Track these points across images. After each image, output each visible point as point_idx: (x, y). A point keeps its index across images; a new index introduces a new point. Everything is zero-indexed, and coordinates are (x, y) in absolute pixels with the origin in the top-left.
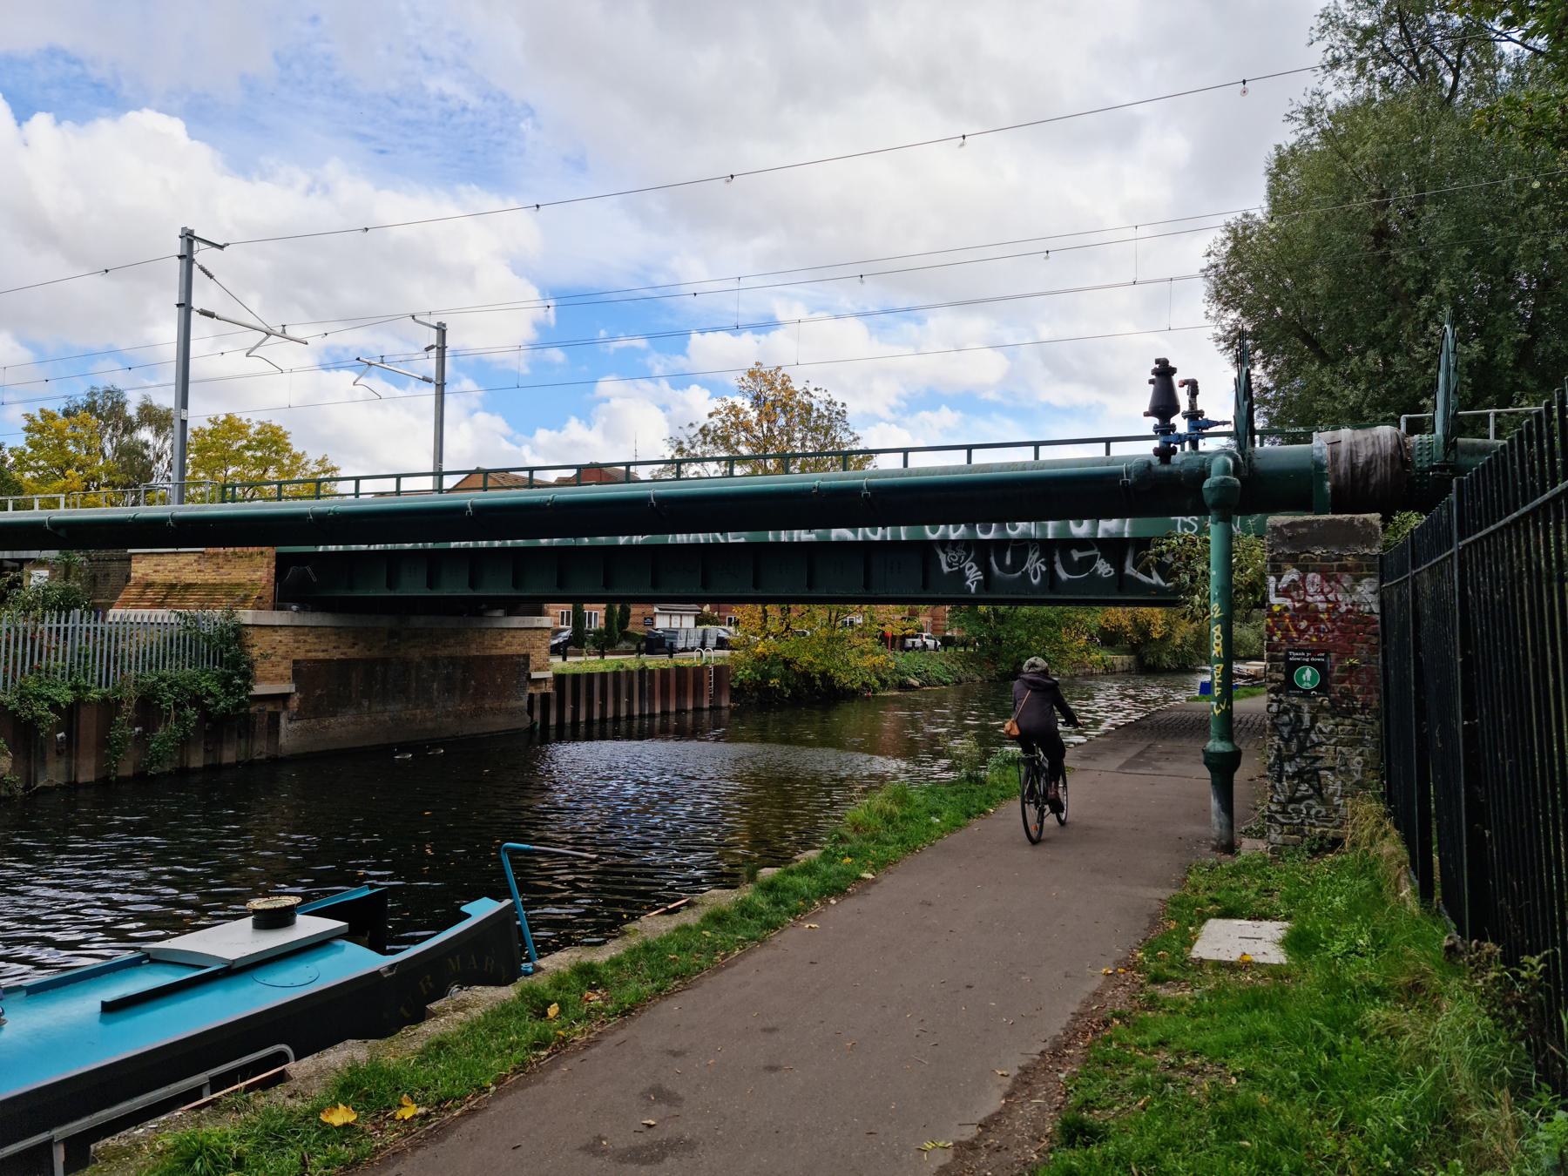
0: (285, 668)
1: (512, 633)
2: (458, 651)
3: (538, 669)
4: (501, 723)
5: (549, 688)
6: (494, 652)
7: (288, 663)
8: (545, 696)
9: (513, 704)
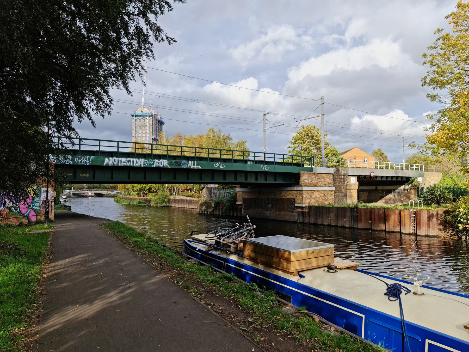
0: (241, 199)
1: (289, 192)
2: (273, 197)
3: (298, 203)
4: (287, 218)
5: (306, 210)
6: (283, 197)
7: (242, 198)
8: (303, 213)
9: (290, 213)
